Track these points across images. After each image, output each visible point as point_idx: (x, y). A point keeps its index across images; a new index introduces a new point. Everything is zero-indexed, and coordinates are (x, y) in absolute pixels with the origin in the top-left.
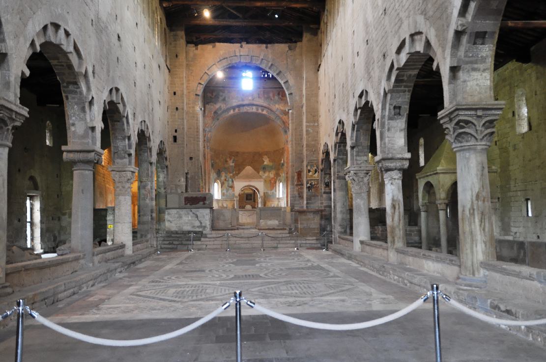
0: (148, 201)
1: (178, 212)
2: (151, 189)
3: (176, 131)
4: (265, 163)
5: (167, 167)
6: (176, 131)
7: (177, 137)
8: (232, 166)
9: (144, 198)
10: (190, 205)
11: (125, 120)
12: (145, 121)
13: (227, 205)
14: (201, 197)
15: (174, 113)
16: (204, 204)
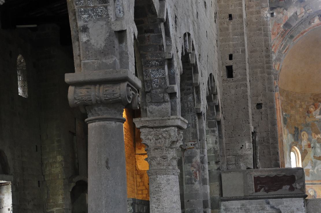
0: (197, 185)
1: (243, 205)
2: (202, 162)
3: (231, 57)
5: (219, 123)
6: (231, 57)
7: (234, 68)
9: (191, 179)
10: (267, 191)
11: (162, 26)
12: (189, 34)
13: (315, 192)
14: (284, 176)
15: (226, 26)
16: (292, 189)
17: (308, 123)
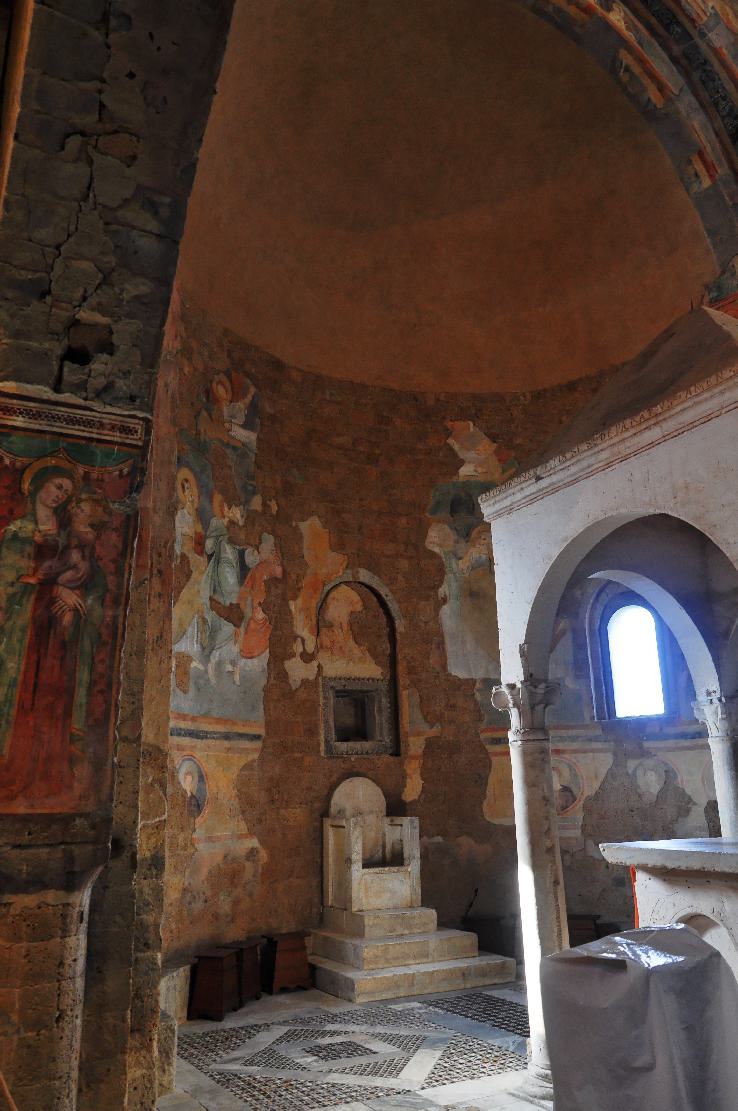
4: (466, 471)
8: (241, 450)
17: (205, 441)
